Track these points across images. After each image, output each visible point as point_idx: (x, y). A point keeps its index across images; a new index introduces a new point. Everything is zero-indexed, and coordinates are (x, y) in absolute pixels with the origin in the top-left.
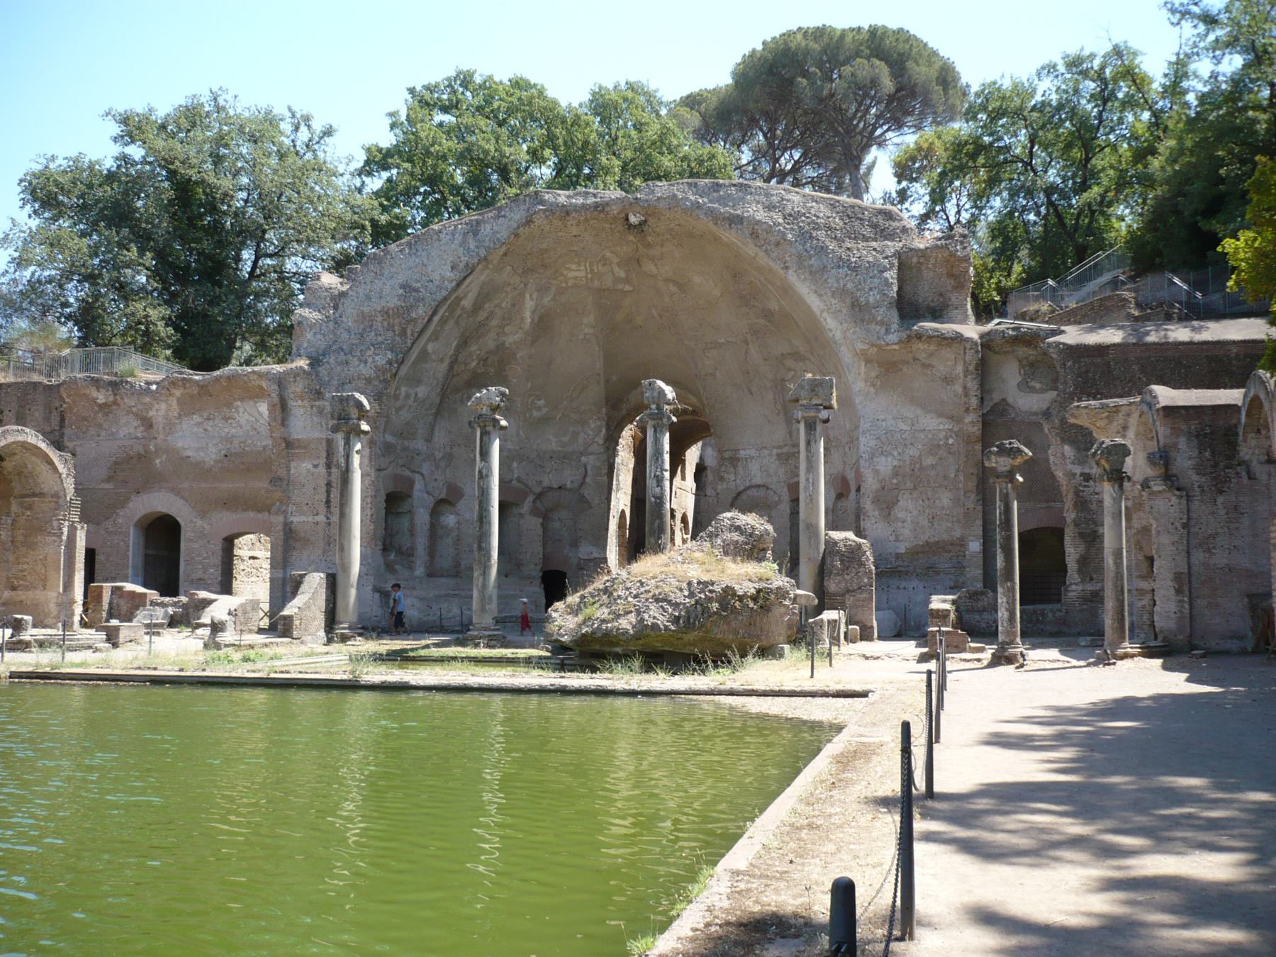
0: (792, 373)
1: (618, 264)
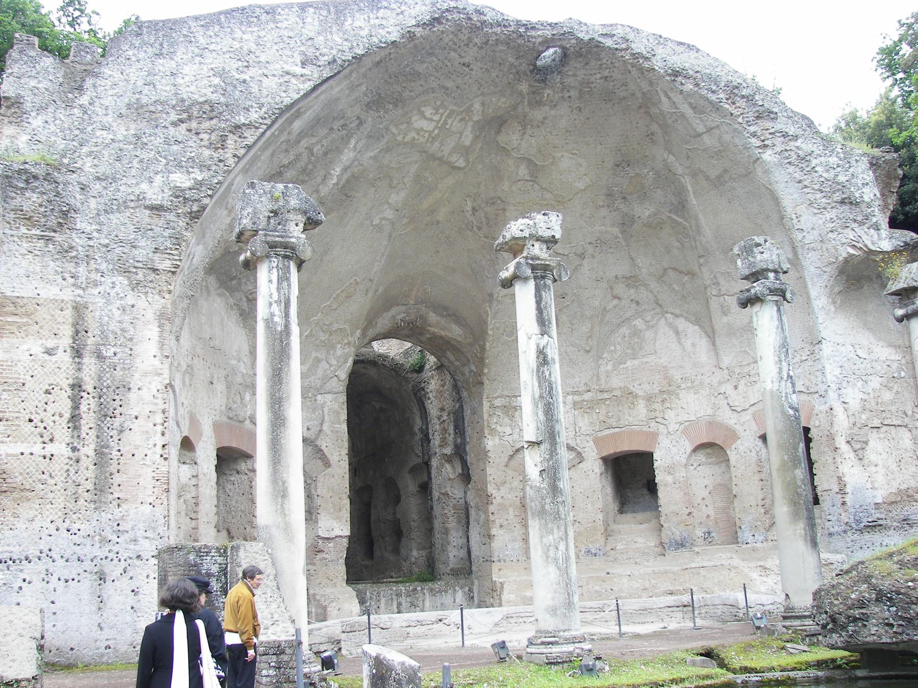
0: (615, 302)
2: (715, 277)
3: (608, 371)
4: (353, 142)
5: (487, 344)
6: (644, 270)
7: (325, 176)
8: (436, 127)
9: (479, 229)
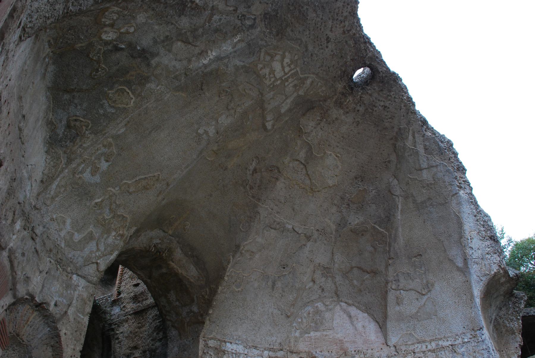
0: (311, 284)
1: (299, 96)
2: (397, 275)
3: (296, 337)
4: (238, 37)
5: (220, 288)
6: (336, 265)
7: (202, 52)
8: (281, 78)
9: (251, 188)
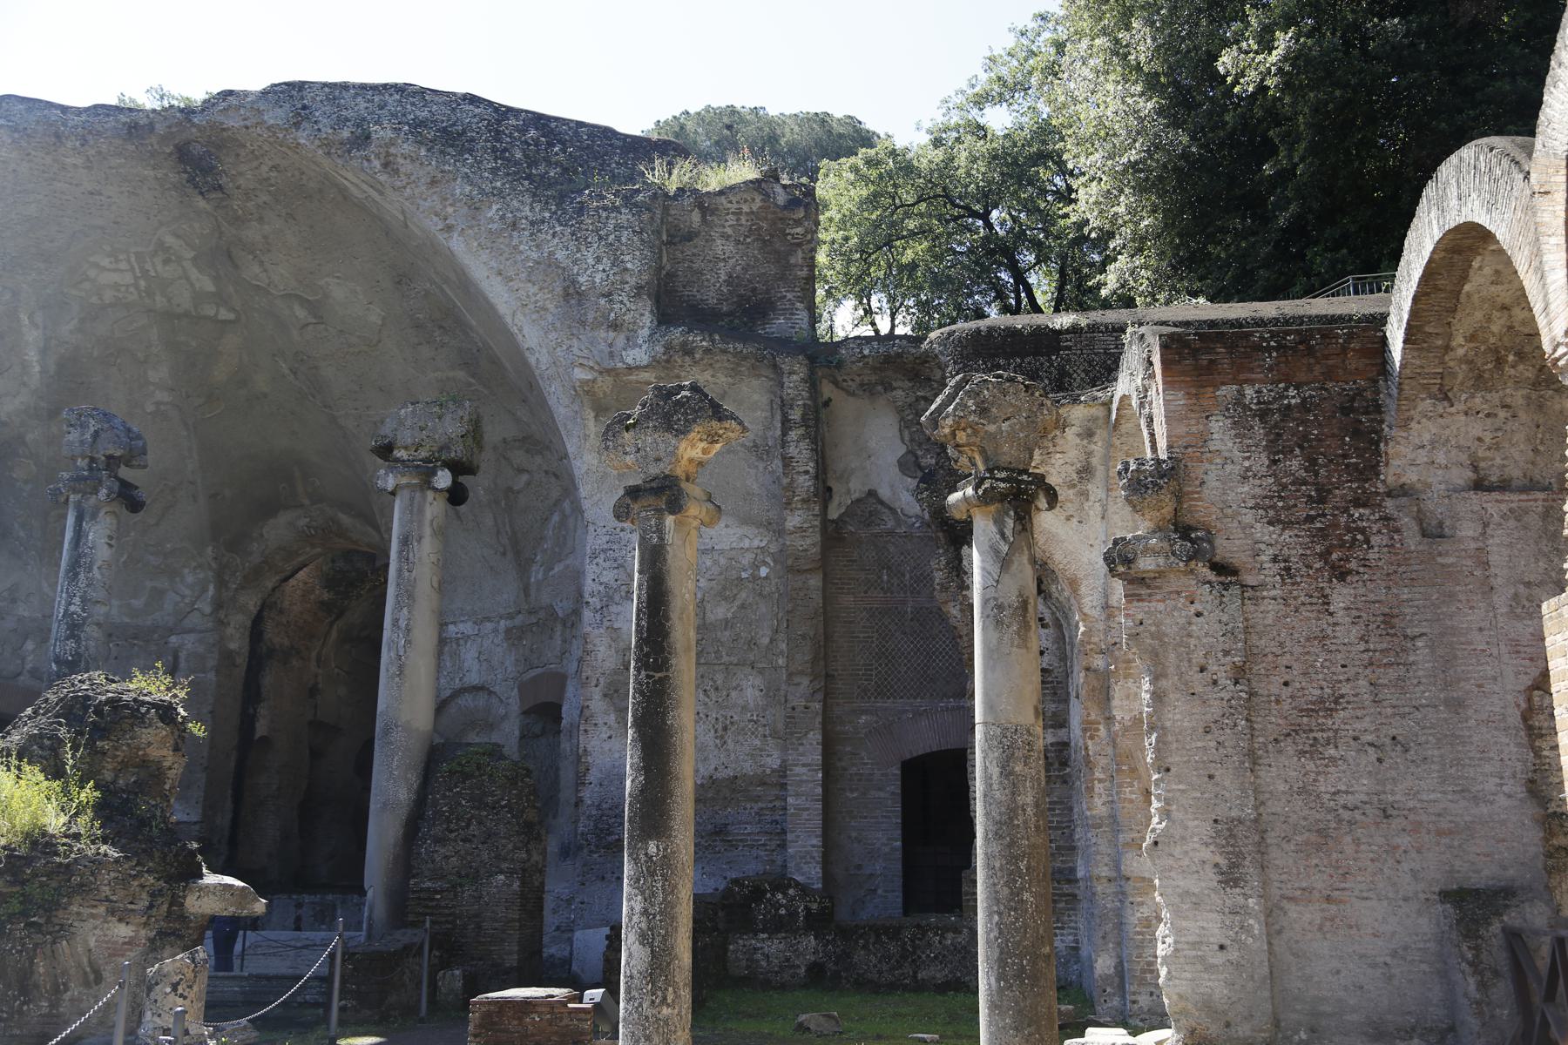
0: (525, 477)
1: (194, 259)
8: (136, 278)
